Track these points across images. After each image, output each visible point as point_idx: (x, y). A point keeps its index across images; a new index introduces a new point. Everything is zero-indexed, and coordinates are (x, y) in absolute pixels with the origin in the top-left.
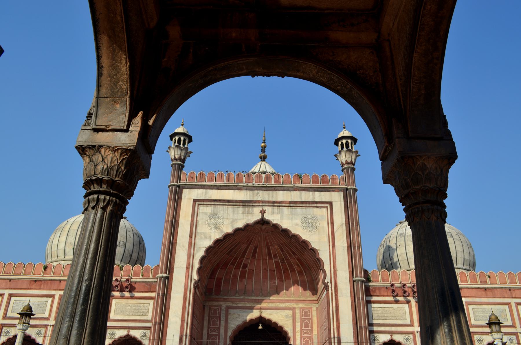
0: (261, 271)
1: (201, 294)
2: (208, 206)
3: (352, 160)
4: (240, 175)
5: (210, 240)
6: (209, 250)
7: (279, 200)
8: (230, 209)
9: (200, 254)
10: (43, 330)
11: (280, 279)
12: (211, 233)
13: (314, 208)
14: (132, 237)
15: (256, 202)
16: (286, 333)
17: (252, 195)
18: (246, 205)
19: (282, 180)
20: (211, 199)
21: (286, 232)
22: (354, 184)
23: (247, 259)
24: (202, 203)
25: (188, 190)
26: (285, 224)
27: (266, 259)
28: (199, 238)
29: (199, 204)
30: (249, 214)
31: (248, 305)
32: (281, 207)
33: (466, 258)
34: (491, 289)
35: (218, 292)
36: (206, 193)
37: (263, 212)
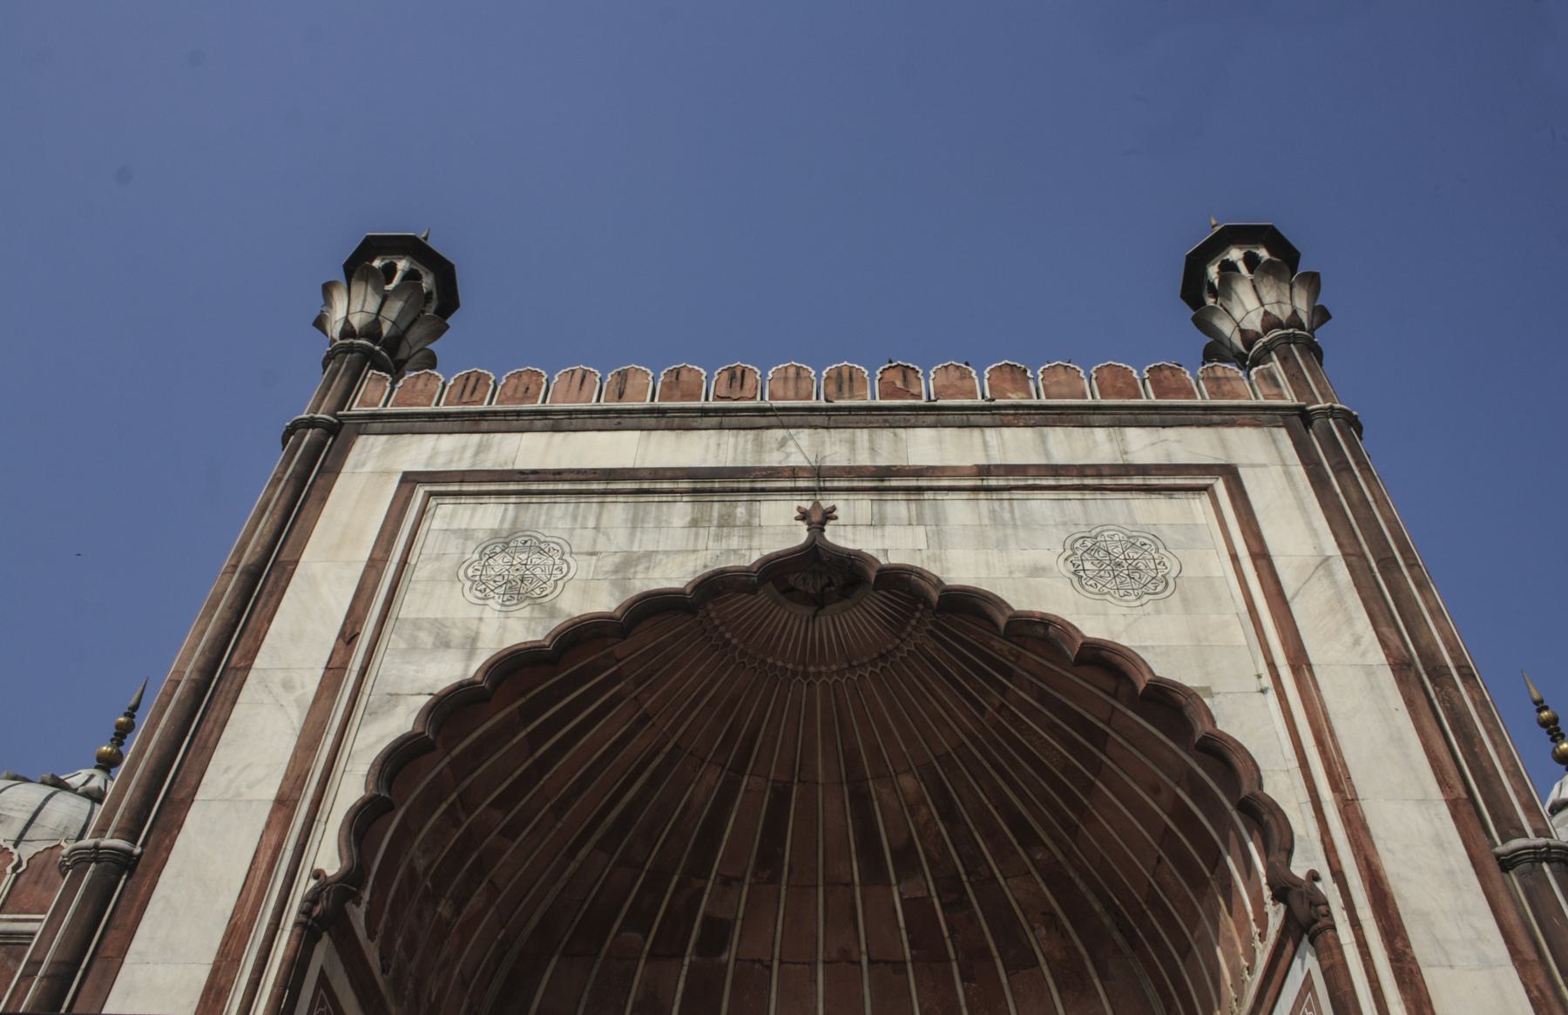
0: (820, 967)
2: (485, 499)
3: (1295, 312)
7: (911, 463)
12: (481, 619)
13: (1135, 495)
15: (773, 473)
17: (749, 446)
18: (712, 491)
20: (509, 467)
23: (726, 881)
27: (850, 884)
28: (403, 645)
29: (431, 494)
30: (734, 526)
32: (928, 495)
37: (818, 520)
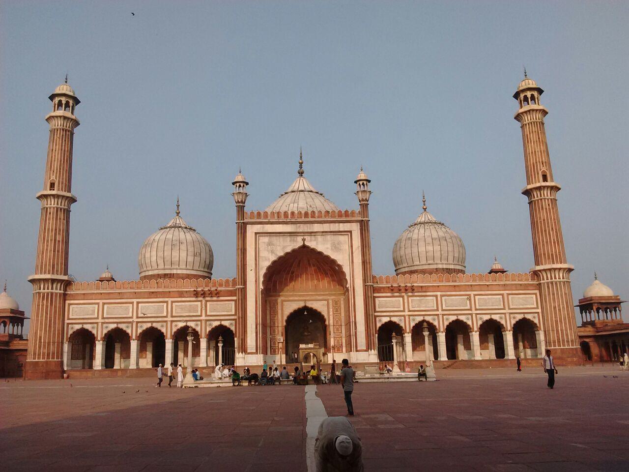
1: (264, 295)
4: (286, 213)
5: (269, 261)
6: (269, 268)
8: (281, 239)
9: (263, 272)
10: (165, 324)
11: (318, 279)
14: (204, 247)
15: (299, 233)
16: (323, 316)
19: (317, 215)
21: (320, 253)
22: (367, 217)
24: (261, 235)
25: (250, 225)
26: (320, 248)
31: (296, 298)
33: (455, 256)
34: (458, 286)
35: (275, 290)
36: (263, 228)
37: (304, 240)
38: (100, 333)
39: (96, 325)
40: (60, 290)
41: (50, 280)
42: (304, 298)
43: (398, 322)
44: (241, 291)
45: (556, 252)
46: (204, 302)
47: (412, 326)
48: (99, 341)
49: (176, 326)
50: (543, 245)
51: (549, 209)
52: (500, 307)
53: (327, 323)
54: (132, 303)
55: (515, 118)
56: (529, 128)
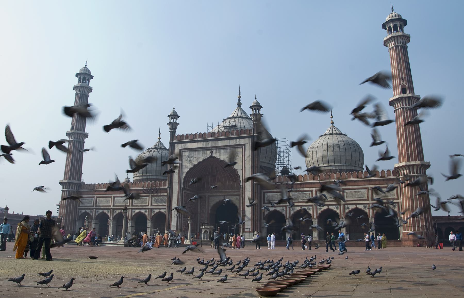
9: (184, 175)
16: (236, 207)
38: (94, 215)
39: (92, 210)
40: (74, 189)
41: (67, 183)
42: (223, 194)
43: (281, 211)
44: (170, 189)
45: (411, 152)
46: (150, 197)
47: (291, 214)
48: (93, 220)
49: (134, 212)
50: (402, 146)
51: (407, 116)
52: (364, 198)
53: (239, 211)
54: (111, 197)
55: (384, 45)
56: (392, 51)
